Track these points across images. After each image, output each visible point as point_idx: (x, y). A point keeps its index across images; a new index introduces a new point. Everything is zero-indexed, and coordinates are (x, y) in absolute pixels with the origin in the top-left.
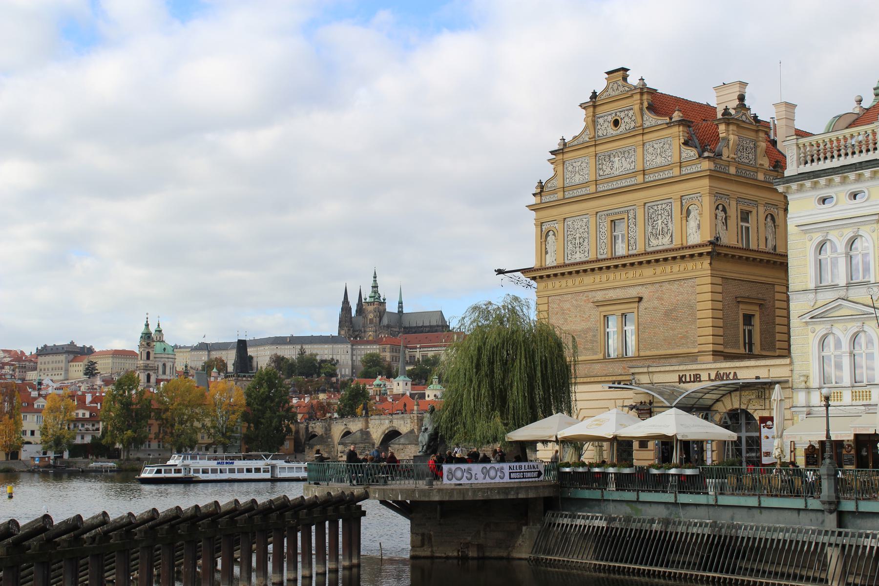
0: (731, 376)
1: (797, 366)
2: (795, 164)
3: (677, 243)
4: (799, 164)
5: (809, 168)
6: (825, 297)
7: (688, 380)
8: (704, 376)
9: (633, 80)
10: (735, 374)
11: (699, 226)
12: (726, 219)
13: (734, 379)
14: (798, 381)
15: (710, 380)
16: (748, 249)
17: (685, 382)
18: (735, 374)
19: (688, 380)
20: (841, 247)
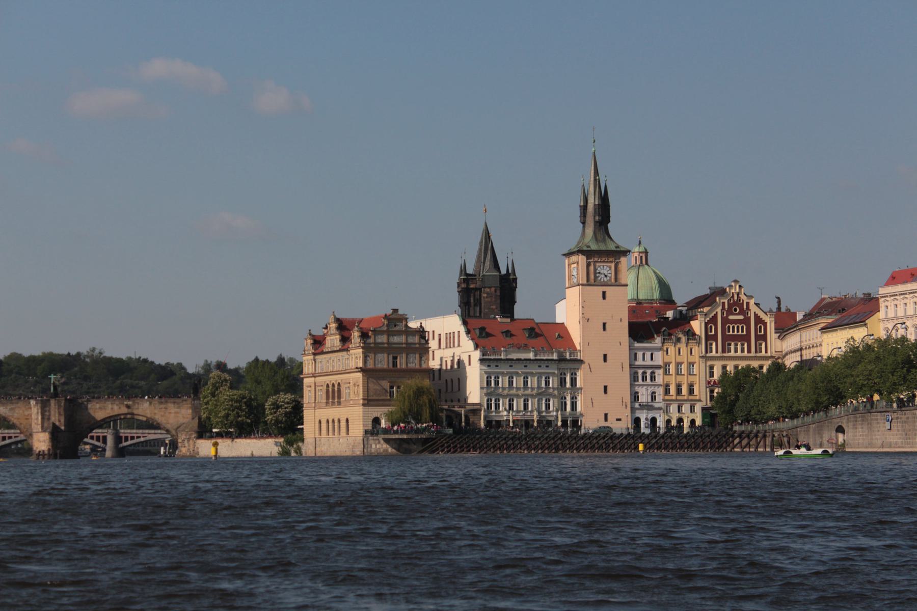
3: (417, 367)
9: (400, 312)
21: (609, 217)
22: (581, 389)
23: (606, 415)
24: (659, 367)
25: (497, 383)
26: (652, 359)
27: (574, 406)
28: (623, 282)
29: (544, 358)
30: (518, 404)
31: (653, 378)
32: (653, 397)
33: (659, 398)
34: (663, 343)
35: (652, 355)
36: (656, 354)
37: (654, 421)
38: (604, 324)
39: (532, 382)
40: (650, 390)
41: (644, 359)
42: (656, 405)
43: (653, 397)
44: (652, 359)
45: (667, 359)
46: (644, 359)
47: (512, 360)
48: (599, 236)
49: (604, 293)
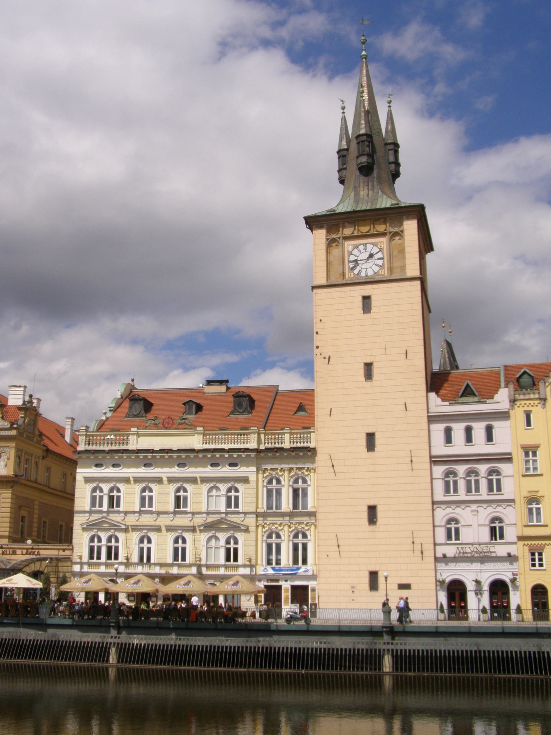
0: (36, 553)
1: (75, 550)
2: (83, 444)
4: (85, 445)
5: (90, 448)
6: (95, 517)
7: (8, 553)
8: (19, 552)
10: (38, 552)
11: (6, 465)
12: (19, 462)
13: (37, 555)
14: (76, 559)
15: (22, 554)
16: (36, 482)
17: (7, 554)
18: (38, 552)
19: (8, 553)
20: (106, 491)
21: (397, 164)
22: (313, 514)
23: (374, 576)
24: (507, 458)
25: (114, 501)
26: (489, 438)
27: (300, 554)
28: (409, 274)
29: (226, 447)
30: (162, 548)
31: (494, 485)
32: (496, 533)
33: (510, 534)
34: (513, 401)
35: (489, 430)
36: (500, 428)
37: (499, 589)
38: (368, 366)
39: (198, 497)
40: (485, 514)
41: (469, 439)
42: (501, 550)
43: (496, 533)
44: (489, 438)
45: (529, 438)
46: (469, 439)
47: (152, 451)
48: (363, 193)
49: (366, 299)
